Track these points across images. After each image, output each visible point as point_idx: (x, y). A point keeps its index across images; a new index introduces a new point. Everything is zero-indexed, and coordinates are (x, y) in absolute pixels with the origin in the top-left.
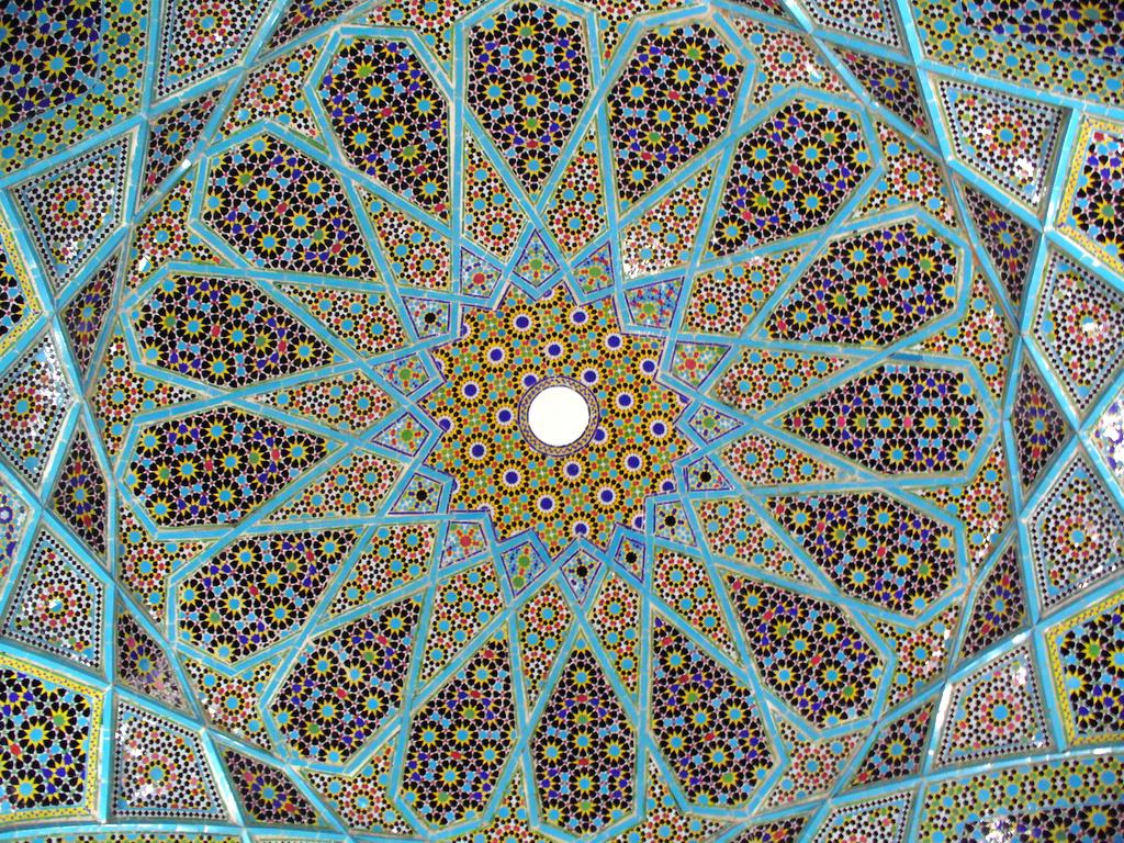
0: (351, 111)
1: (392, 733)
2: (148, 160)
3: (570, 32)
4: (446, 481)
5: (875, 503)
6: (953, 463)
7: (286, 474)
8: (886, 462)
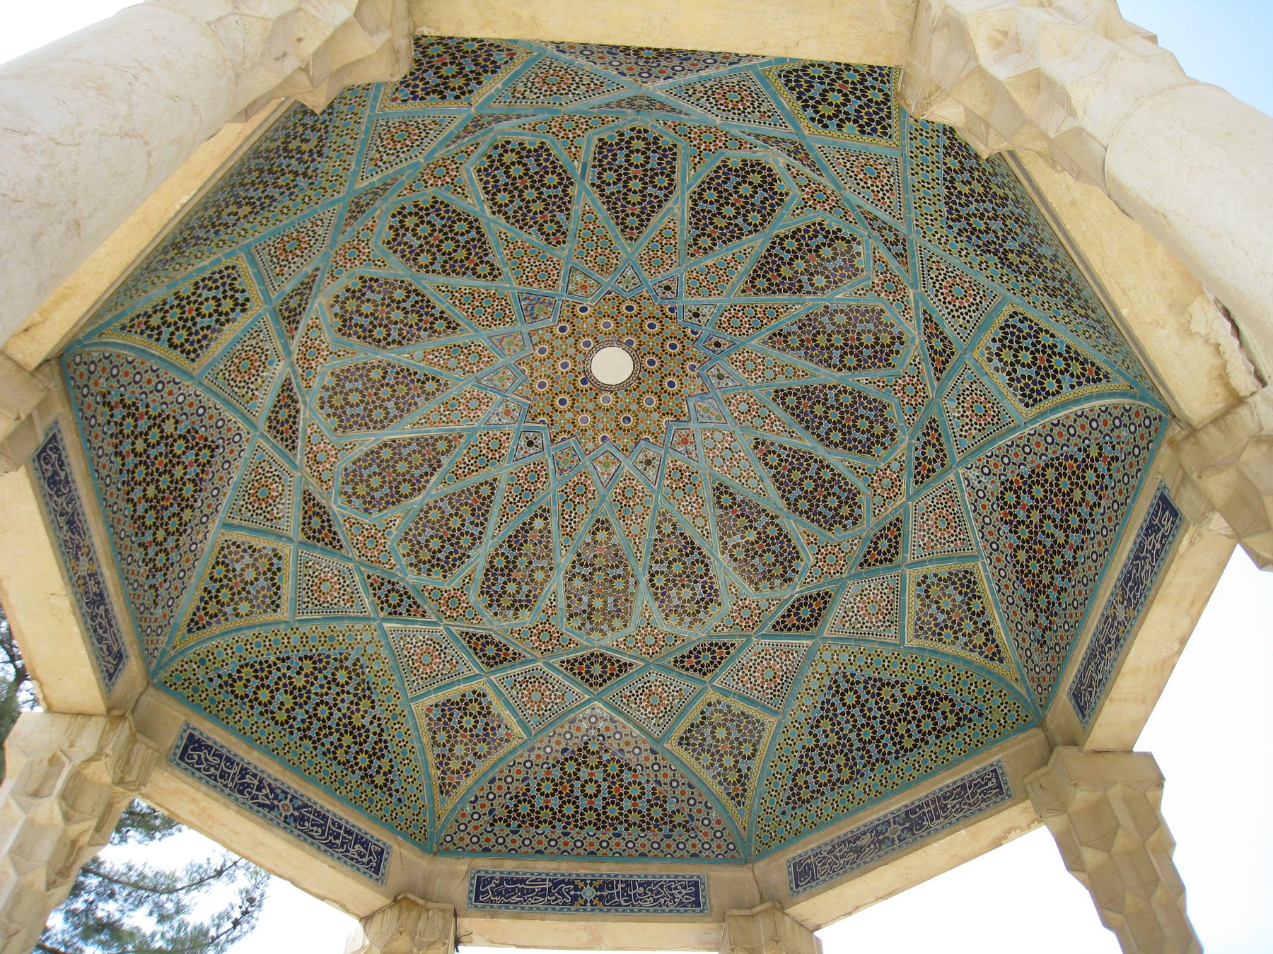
0: (387, 495)
1: (795, 527)
2: (405, 616)
3: (338, 376)
4: (642, 444)
5: (698, 198)
6: (671, 149)
7: (614, 545)
8: (666, 188)
